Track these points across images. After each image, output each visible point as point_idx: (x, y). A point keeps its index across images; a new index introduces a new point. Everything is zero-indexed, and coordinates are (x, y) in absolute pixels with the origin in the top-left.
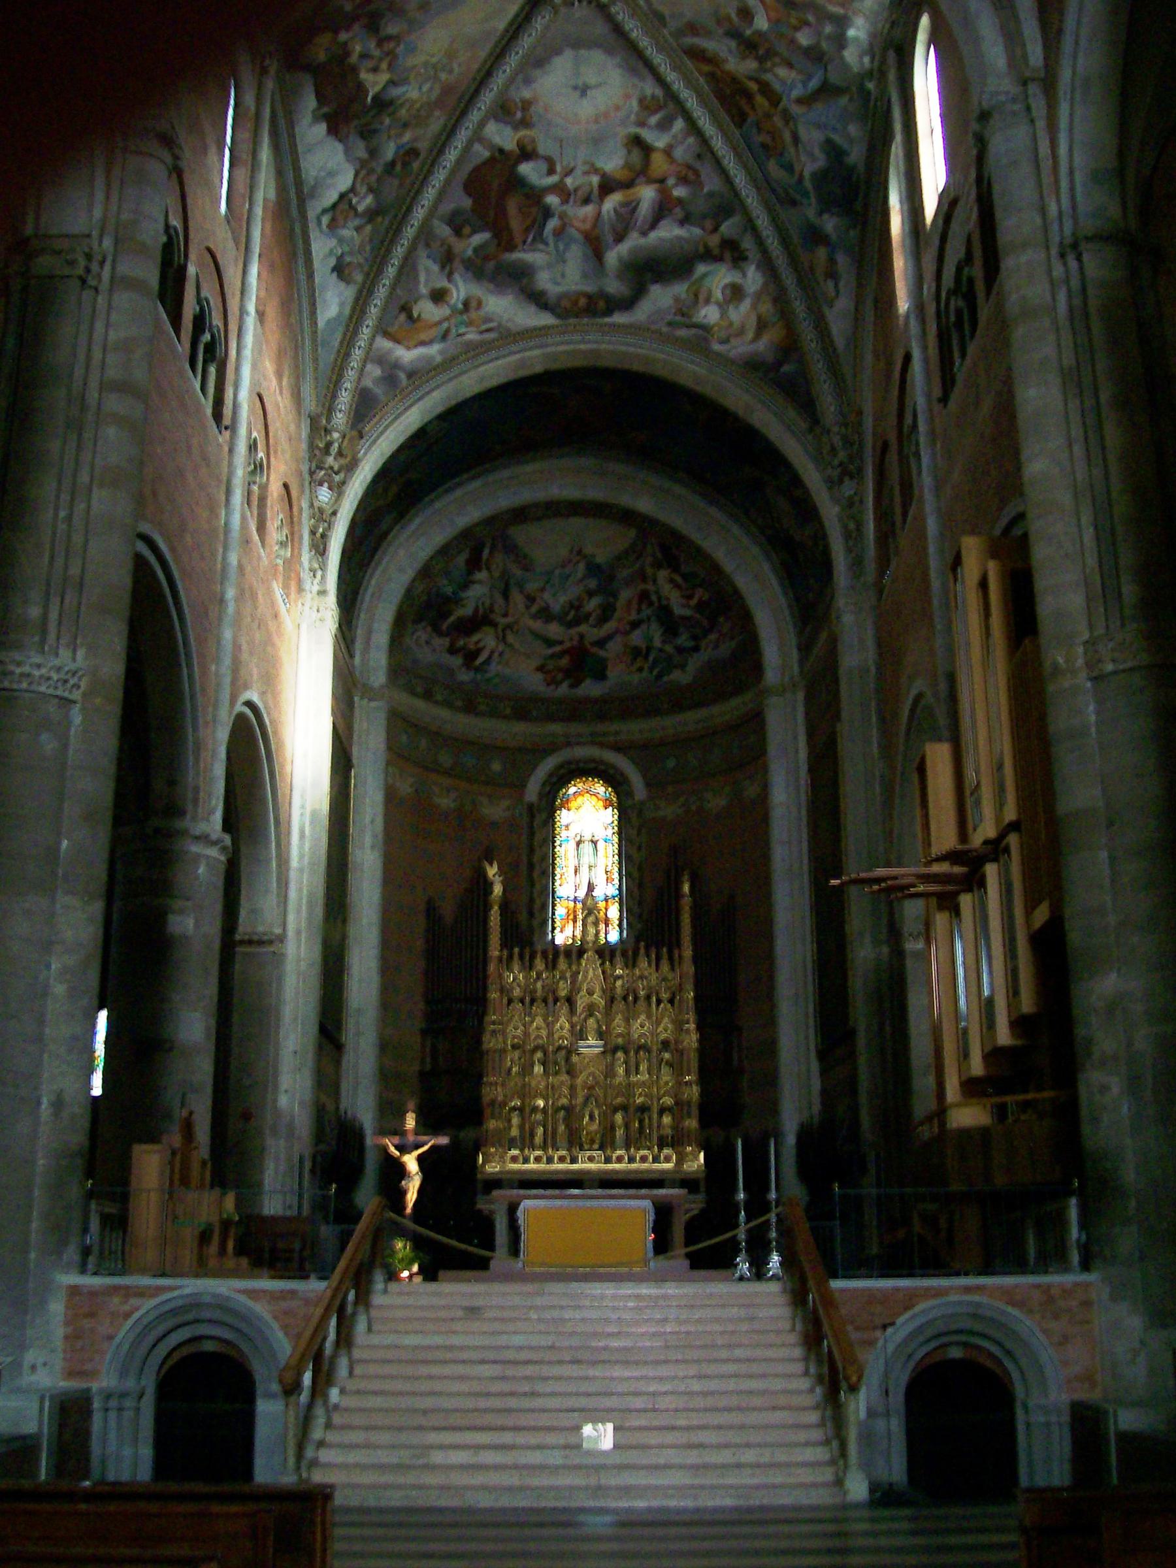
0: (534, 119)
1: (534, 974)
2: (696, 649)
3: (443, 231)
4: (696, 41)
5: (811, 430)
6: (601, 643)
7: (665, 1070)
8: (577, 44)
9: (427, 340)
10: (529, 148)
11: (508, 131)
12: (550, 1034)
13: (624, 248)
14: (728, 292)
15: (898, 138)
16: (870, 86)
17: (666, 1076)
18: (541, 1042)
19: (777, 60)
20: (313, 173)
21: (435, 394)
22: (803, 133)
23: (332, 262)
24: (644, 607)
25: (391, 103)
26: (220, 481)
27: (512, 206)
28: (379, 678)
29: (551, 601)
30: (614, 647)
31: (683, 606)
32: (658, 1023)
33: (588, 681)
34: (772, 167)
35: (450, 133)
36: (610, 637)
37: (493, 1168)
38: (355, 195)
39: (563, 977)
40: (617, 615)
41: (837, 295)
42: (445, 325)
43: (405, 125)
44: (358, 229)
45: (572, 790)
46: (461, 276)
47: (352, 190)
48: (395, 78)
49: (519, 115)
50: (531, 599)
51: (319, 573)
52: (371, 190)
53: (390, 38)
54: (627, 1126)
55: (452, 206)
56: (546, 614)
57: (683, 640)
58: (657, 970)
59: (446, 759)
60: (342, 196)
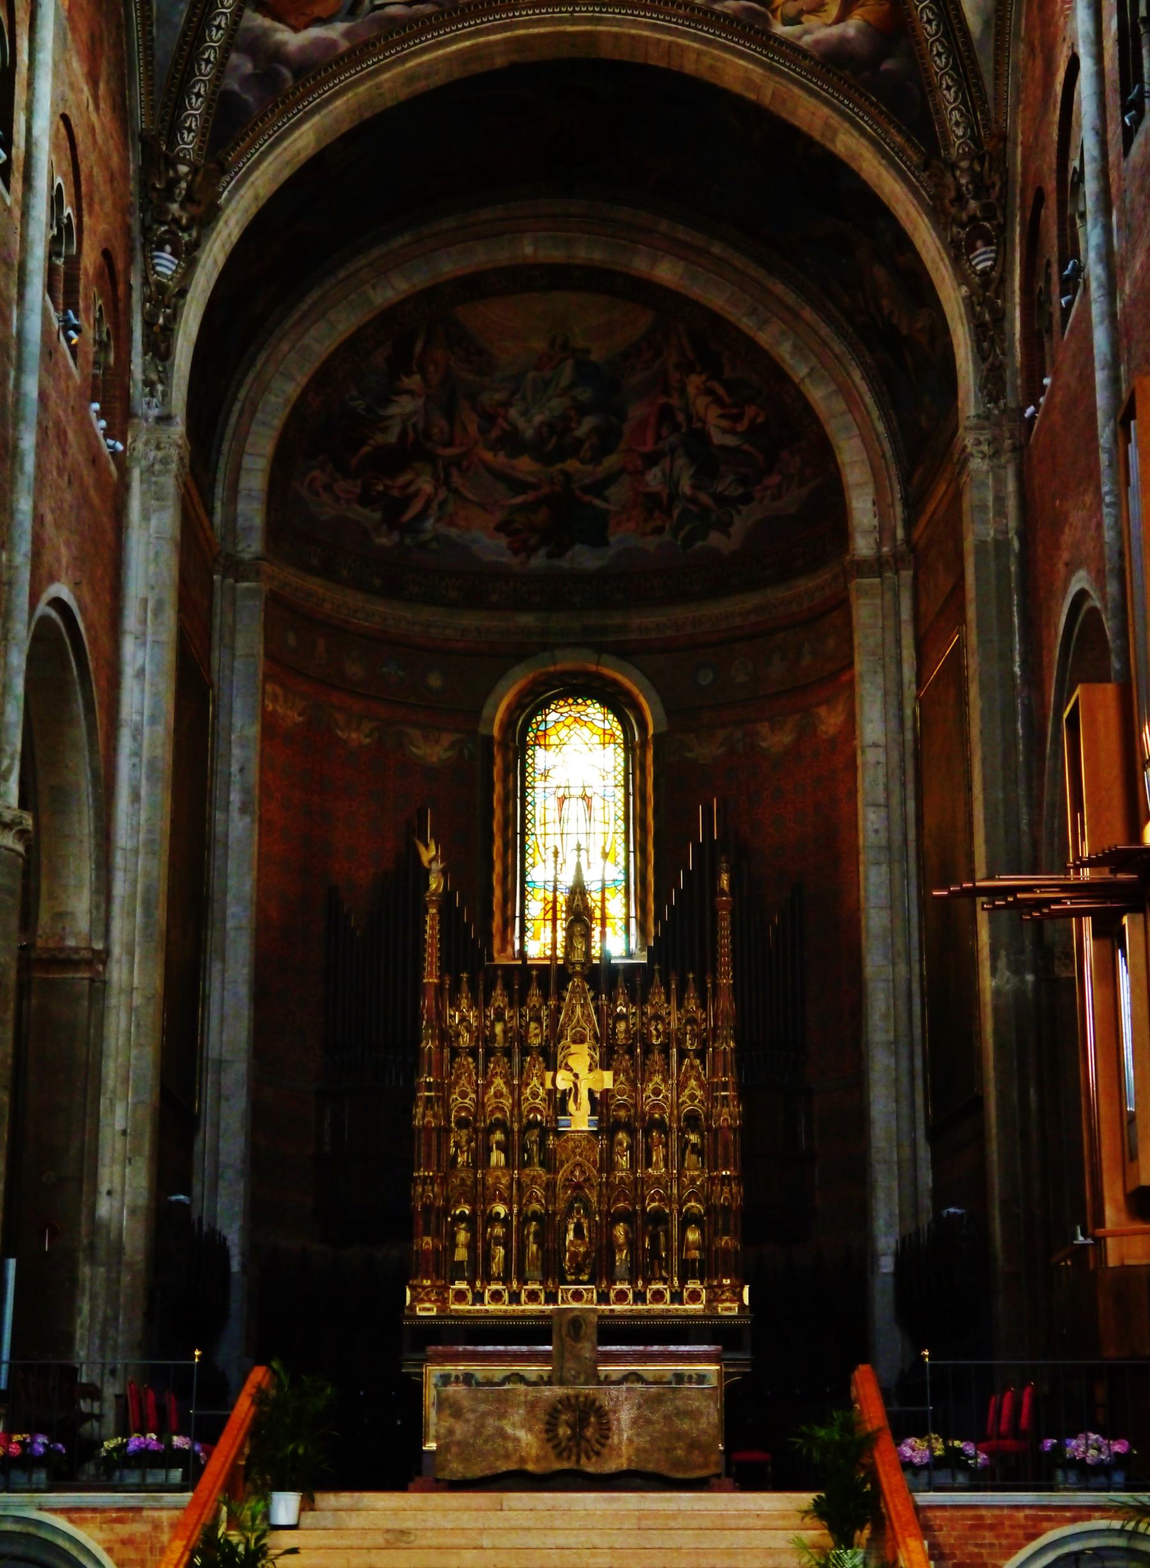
1: (491, 1013)
2: (746, 499)
5: (926, 166)
6: (599, 487)
7: (691, 1159)
9: (324, 16)
12: (517, 1104)
17: (694, 1168)
18: (498, 1115)
21: (338, 103)
24: (665, 431)
26: (8, 264)
28: (252, 546)
29: (521, 423)
30: (618, 493)
31: (725, 431)
32: (681, 1086)
33: (578, 547)
36: (611, 479)
37: (427, 1310)
39: (538, 1020)
40: (622, 446)
45: (552, 717)
50: (489, 418)
51: (160, 387)
54: (632, 1244)
56: (512, 443)
57: (727, 485)
58: (680, 1006)
59: (355, 670)
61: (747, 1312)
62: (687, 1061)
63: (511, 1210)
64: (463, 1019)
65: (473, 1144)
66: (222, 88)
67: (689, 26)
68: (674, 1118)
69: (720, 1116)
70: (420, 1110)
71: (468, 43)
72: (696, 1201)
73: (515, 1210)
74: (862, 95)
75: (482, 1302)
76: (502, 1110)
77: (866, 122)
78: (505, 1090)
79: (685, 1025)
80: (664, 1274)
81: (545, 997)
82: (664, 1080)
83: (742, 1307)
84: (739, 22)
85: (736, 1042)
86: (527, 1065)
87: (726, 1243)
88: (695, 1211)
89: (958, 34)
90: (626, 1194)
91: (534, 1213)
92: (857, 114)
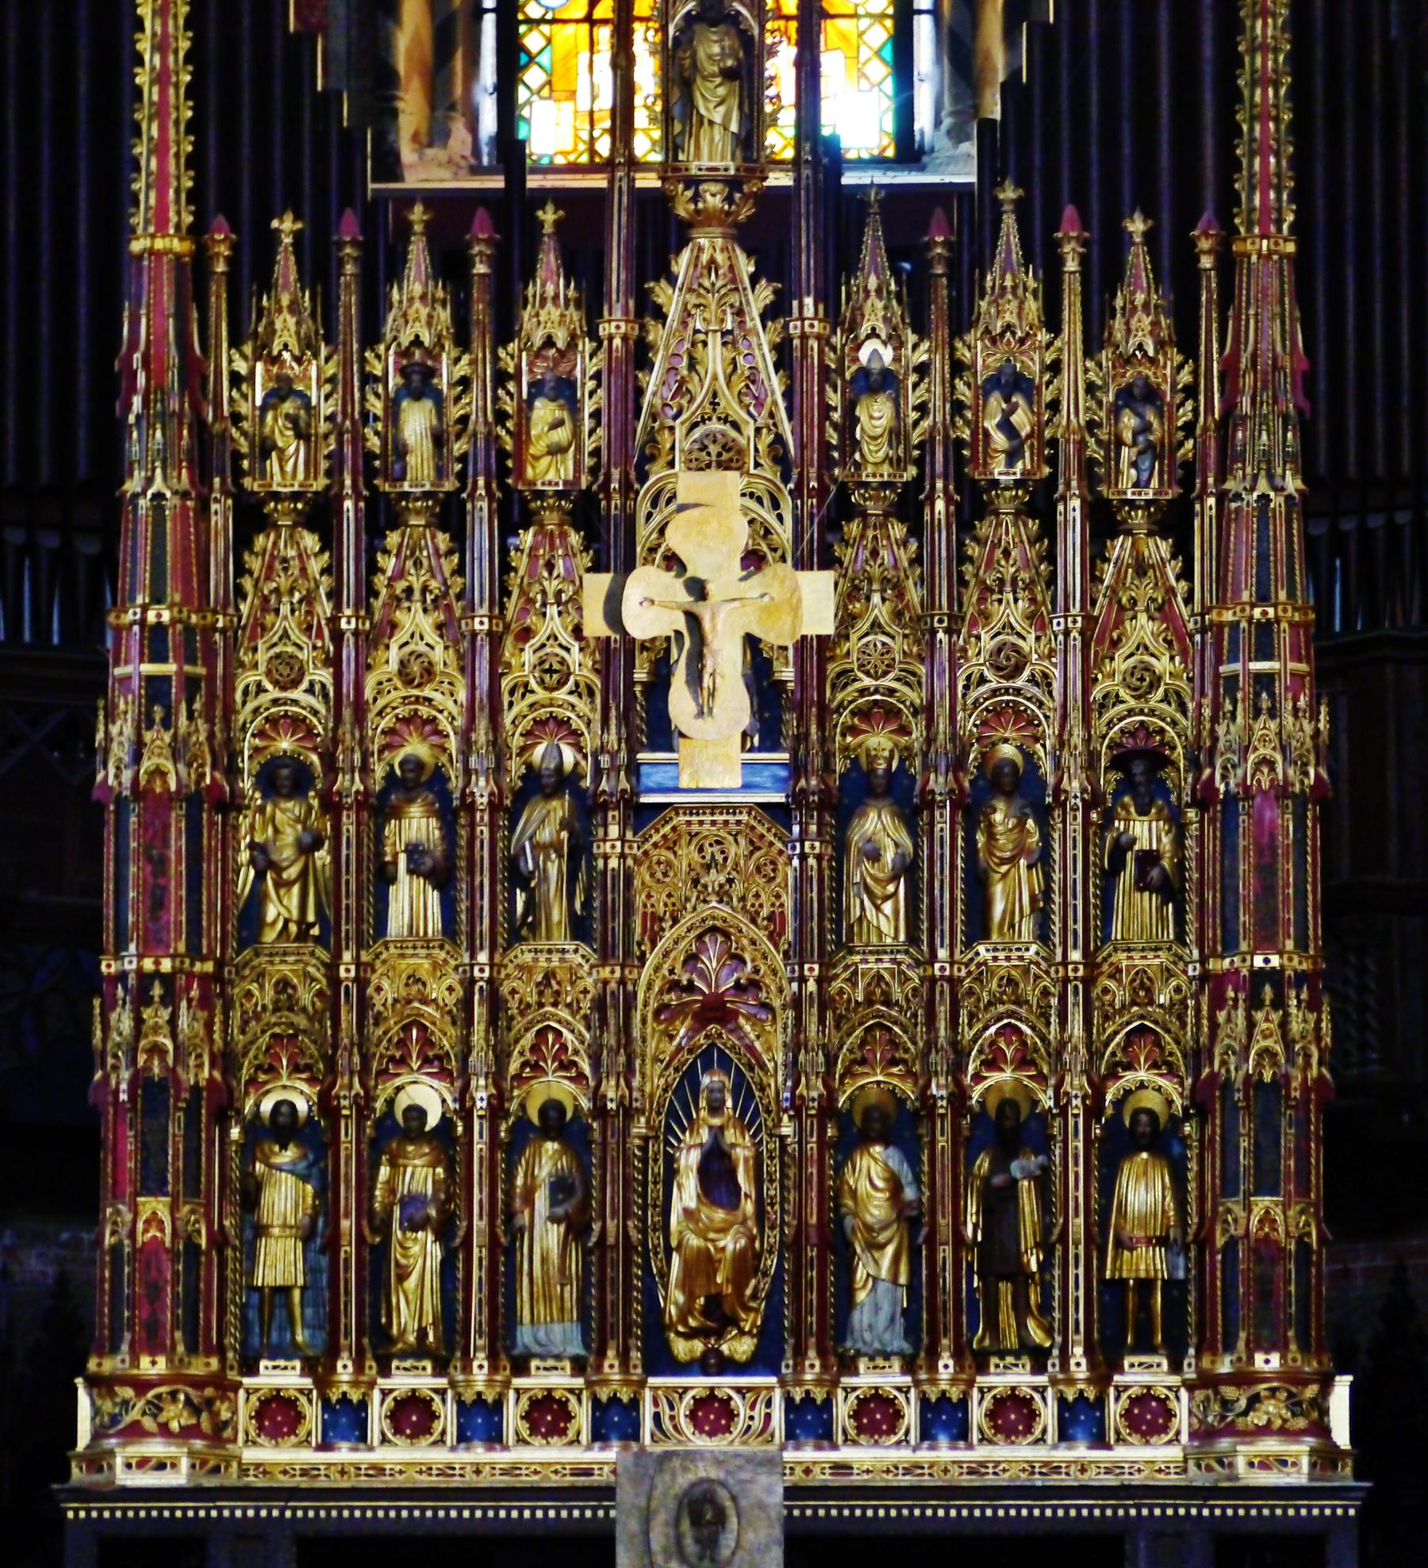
1: (385, 363)
18: (416, 747)
39: (565, 391)
58: (1093, 344)
61: (1345, 1476)
62: (1119, 548)
63: (464, 1094)
64: (281, 390)
65: (322, 856)
68: (1073, 762)
69: (1245, 751)
70: (122, 730)
72: (1155, 1066)
73: (481, 1094)
75: (359, 1433)
76: (429, 727)
78: (439, 655)
79: (1115, 411)
80: (1037, 1335)
81: (592, 306)
82: (1036, 619)
83: (1326, 1456)
85: (1307, 473)
86: (521, 562)
87: (1267, 1218)
88: (1151, 1100)
90: (894, 1044)
91: (551, 1109)
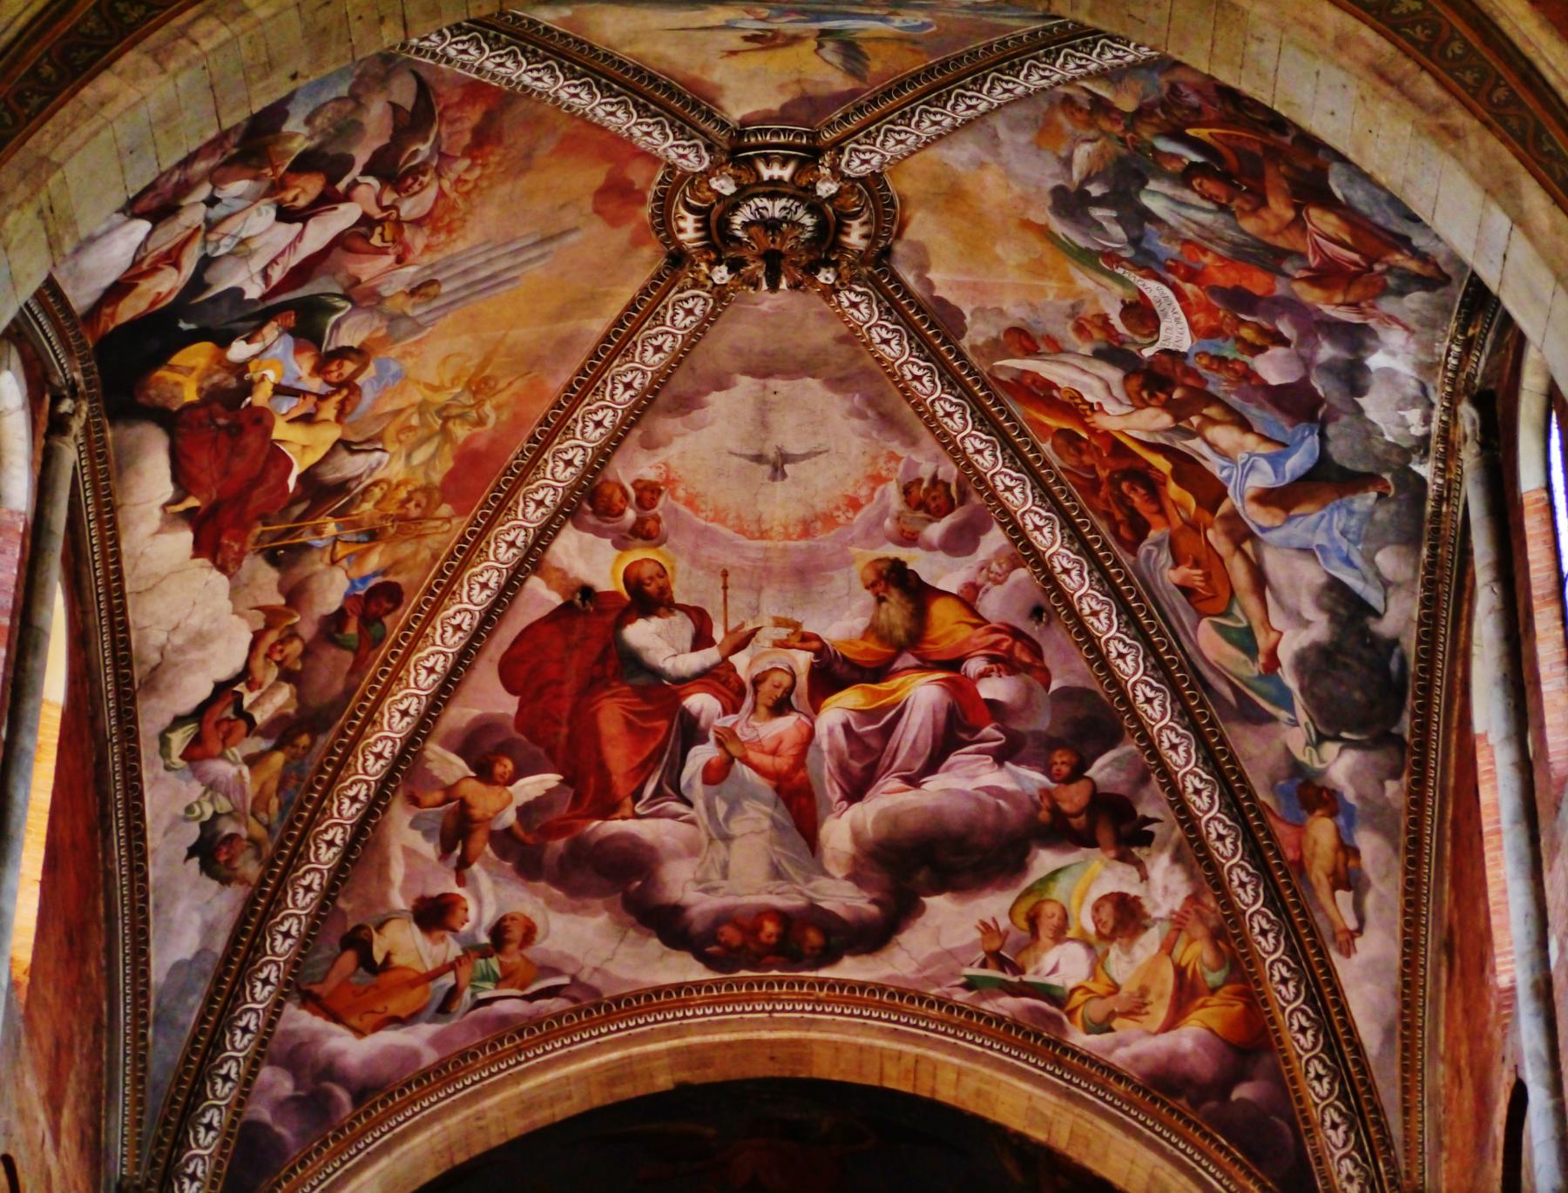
0: (664, 525)
3: (448, 765)
4: (1030, 364)
8: (764, 368)
9: (403, 1015)
10: (652, 588)
11: (604, 548)
13: (868, 812)
14: (1107, 912)
15: (1486, 600)
16: (1425, 470)
19: (1212, 411)
20: (158, 637)
21: (419, 1140)
22: (1273, 563)
23: (193, 832)
25: (342, 487)
27: (611, 717)
34: (1209, 641)
35: (469, 549)
38: (251, 686)
41: (1360, 931)
42: (449, 980)
43: (374, 536)
44: (252, 761)
46: (486, 866)
47: (245, 674)
48: (354, 439)
49: (630, 515)
52: (287, 676)
53: (343, 353)
55: (476, 712)
60: (222, 689)
66: (246, 1116)
67: (945, 1033)
71: (615, 1055)
74: (1205, 1135)
77: (1213, 1175)
84: (1019, 1029)
89: (1346, 1049)
92: (1198, 1163)
